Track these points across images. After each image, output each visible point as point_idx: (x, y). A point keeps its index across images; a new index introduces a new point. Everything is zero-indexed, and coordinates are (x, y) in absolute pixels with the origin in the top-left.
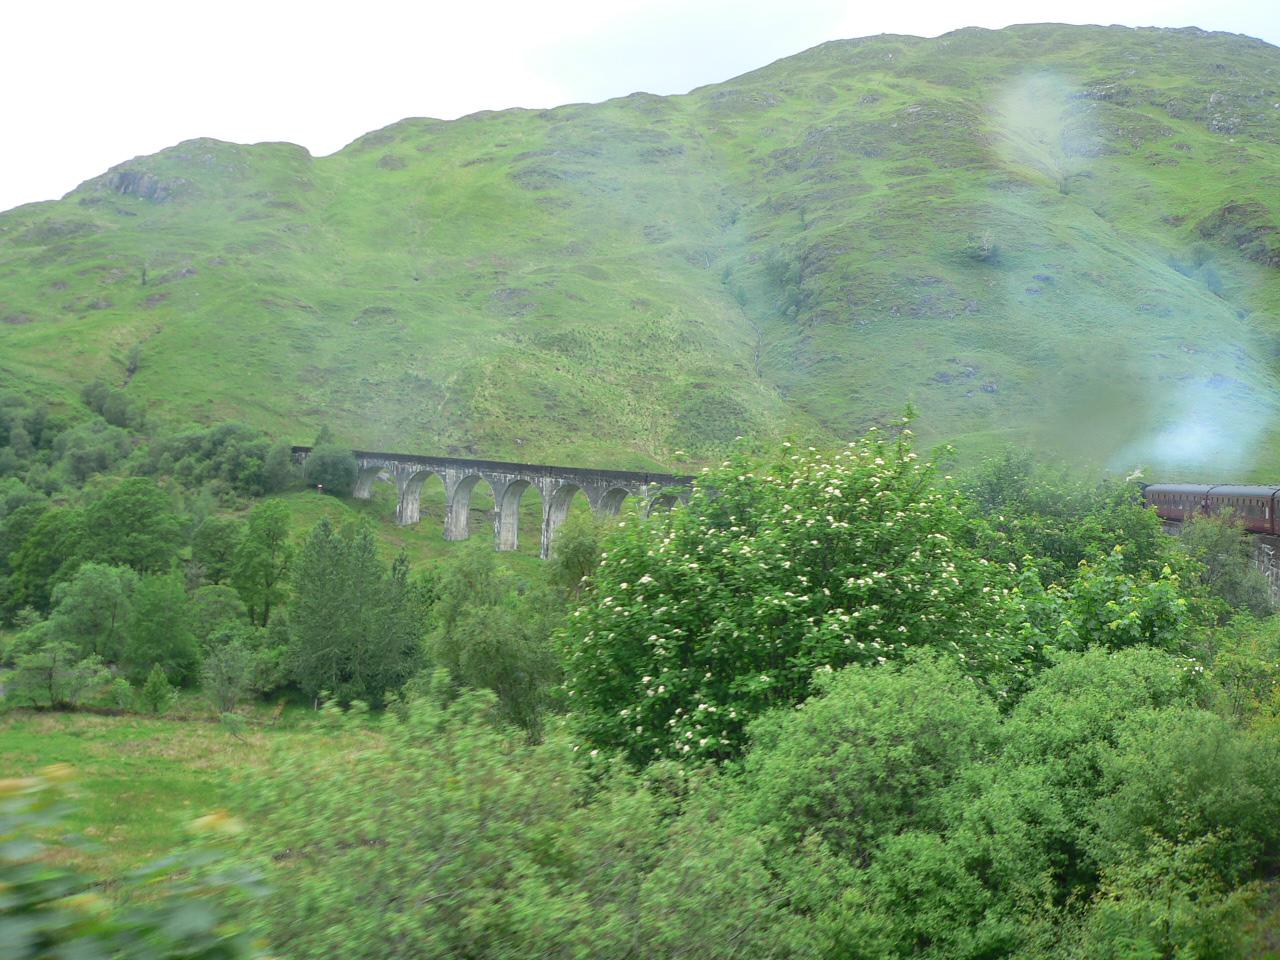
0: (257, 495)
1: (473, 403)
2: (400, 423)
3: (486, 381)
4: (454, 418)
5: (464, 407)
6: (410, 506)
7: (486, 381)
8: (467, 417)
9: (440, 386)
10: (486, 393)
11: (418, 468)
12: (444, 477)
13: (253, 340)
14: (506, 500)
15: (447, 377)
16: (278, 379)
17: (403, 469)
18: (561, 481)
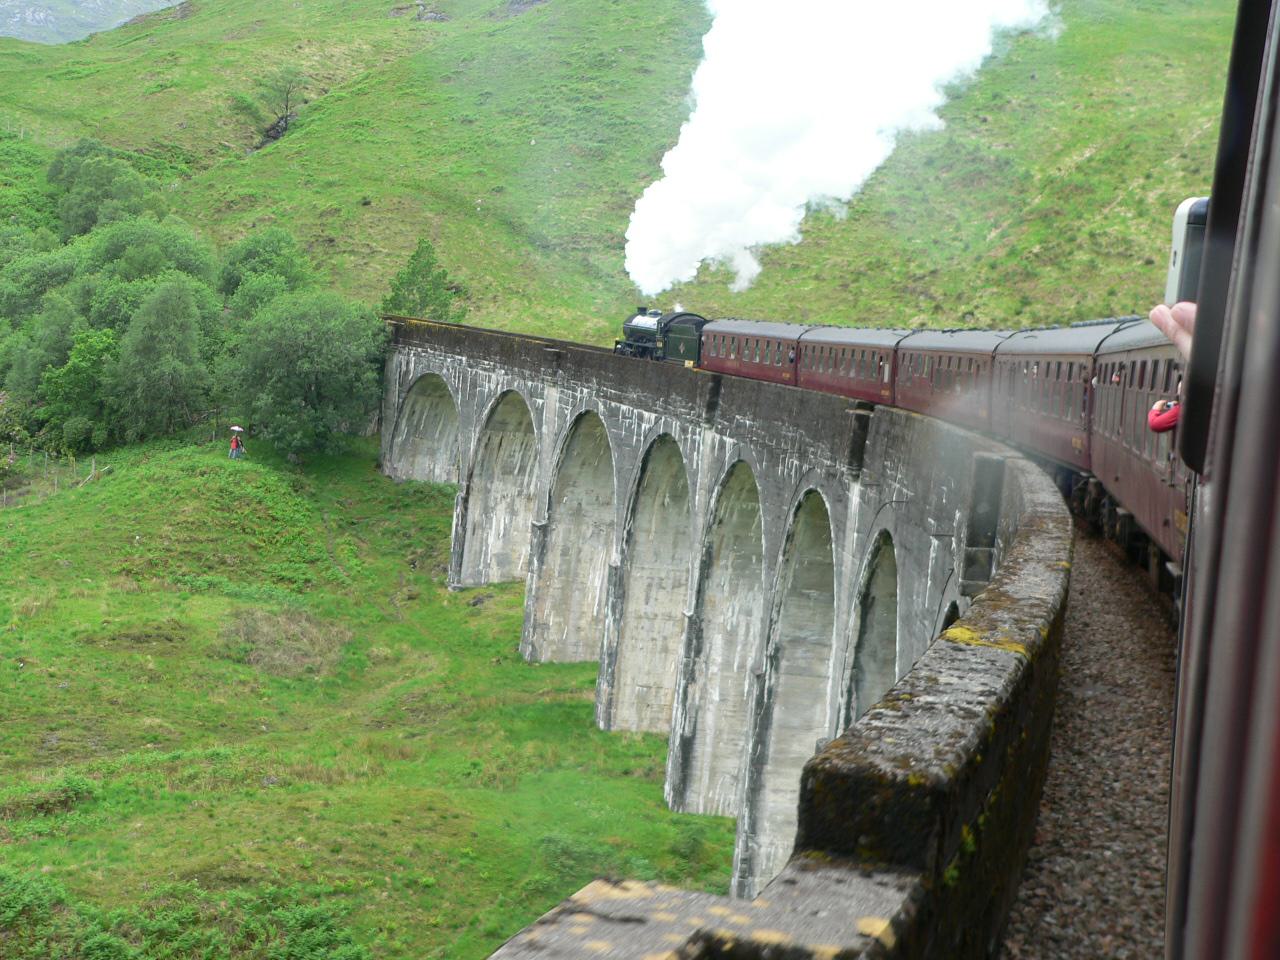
0: (84, 447)
1: (1095, 222)
2: (858, 275)
3: (1174, 162)
4: (1011, 264)
5: (1062, 232)
6: (500, 518)
7: (1174, 162)
8: (1053, 261)
9: (1028, 176)
10: (1151, 197)
11: (495, 379)
12: (540, 411)
13: (601, 63)
14: (649, 519)
15: (1067, 149)
16: (600, 156)
17: (474, 385)
18: (729, 441)
